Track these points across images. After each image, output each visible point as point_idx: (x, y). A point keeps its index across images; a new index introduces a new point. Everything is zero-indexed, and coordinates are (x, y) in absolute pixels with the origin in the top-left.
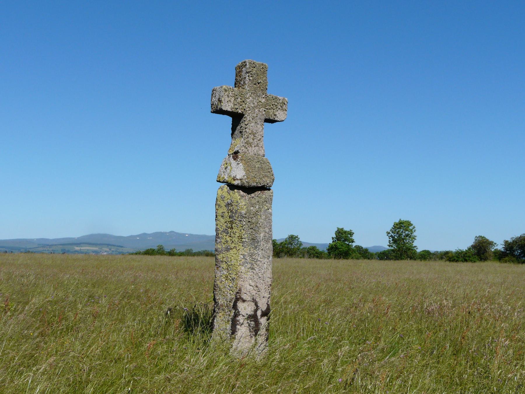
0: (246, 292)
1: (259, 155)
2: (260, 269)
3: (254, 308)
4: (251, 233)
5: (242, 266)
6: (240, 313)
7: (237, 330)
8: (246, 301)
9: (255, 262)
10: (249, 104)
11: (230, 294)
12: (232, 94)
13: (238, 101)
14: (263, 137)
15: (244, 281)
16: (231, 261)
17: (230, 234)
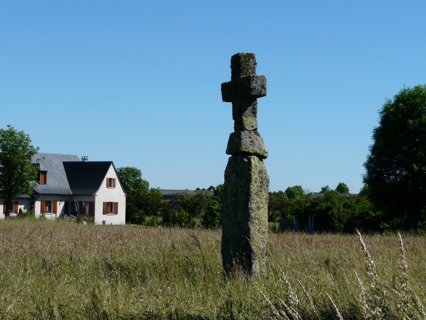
11: (262, 244)
16: (262, 218)
17: (260, 196)
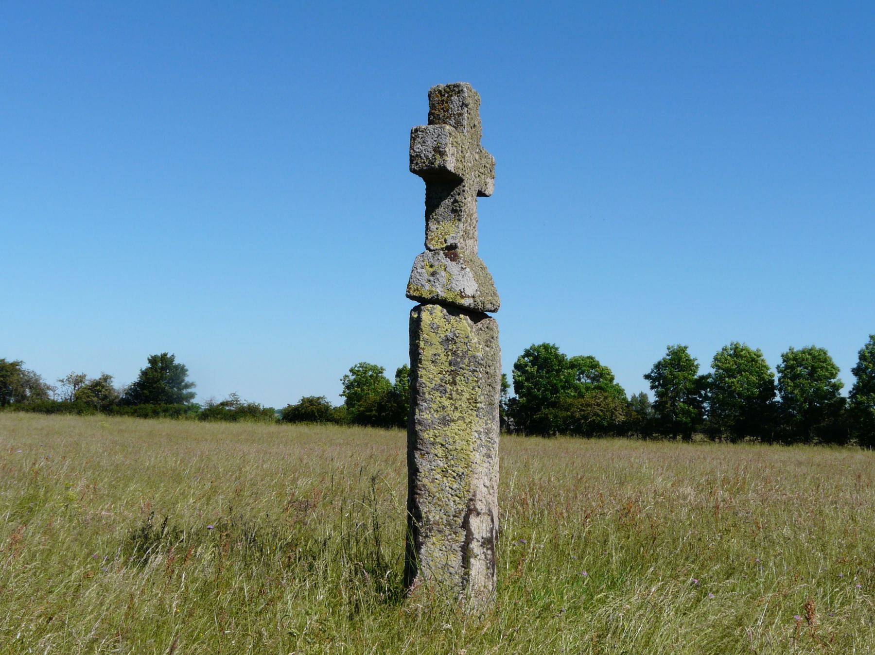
6: (474, 536)
11: (454, 501)
16: (454, 442)
17: (451, 394)
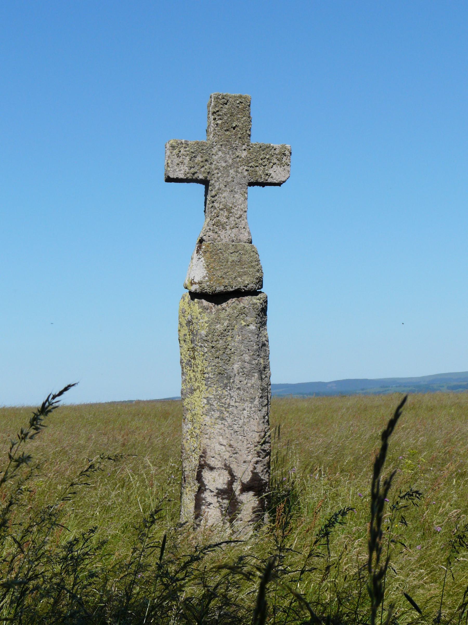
0: (214, 455)
1: (240, 241)
2: (236, 418)
3: (228, 478)
4: (217, 365)
5: (206, 415)
6: (207, 487)
7: (202, 513)
8: (215, 468)
9: (225, 408)
10: (218, 162)
12: (186, 151)
13: (196, 161)
14: (245, 212)
15: (210, 439)
